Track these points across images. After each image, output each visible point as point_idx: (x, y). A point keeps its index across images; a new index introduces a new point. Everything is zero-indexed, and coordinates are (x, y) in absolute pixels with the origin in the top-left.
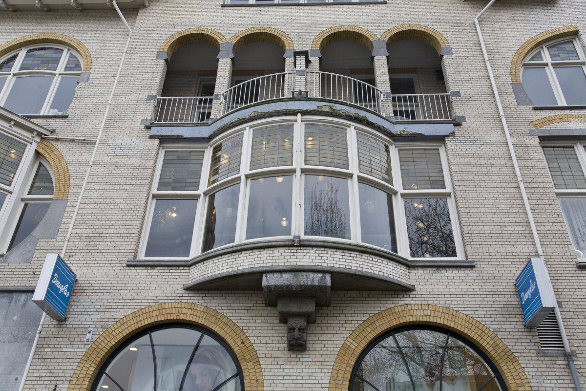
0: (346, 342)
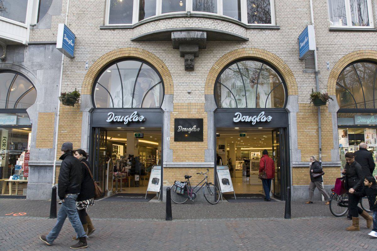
0: (214, 66)
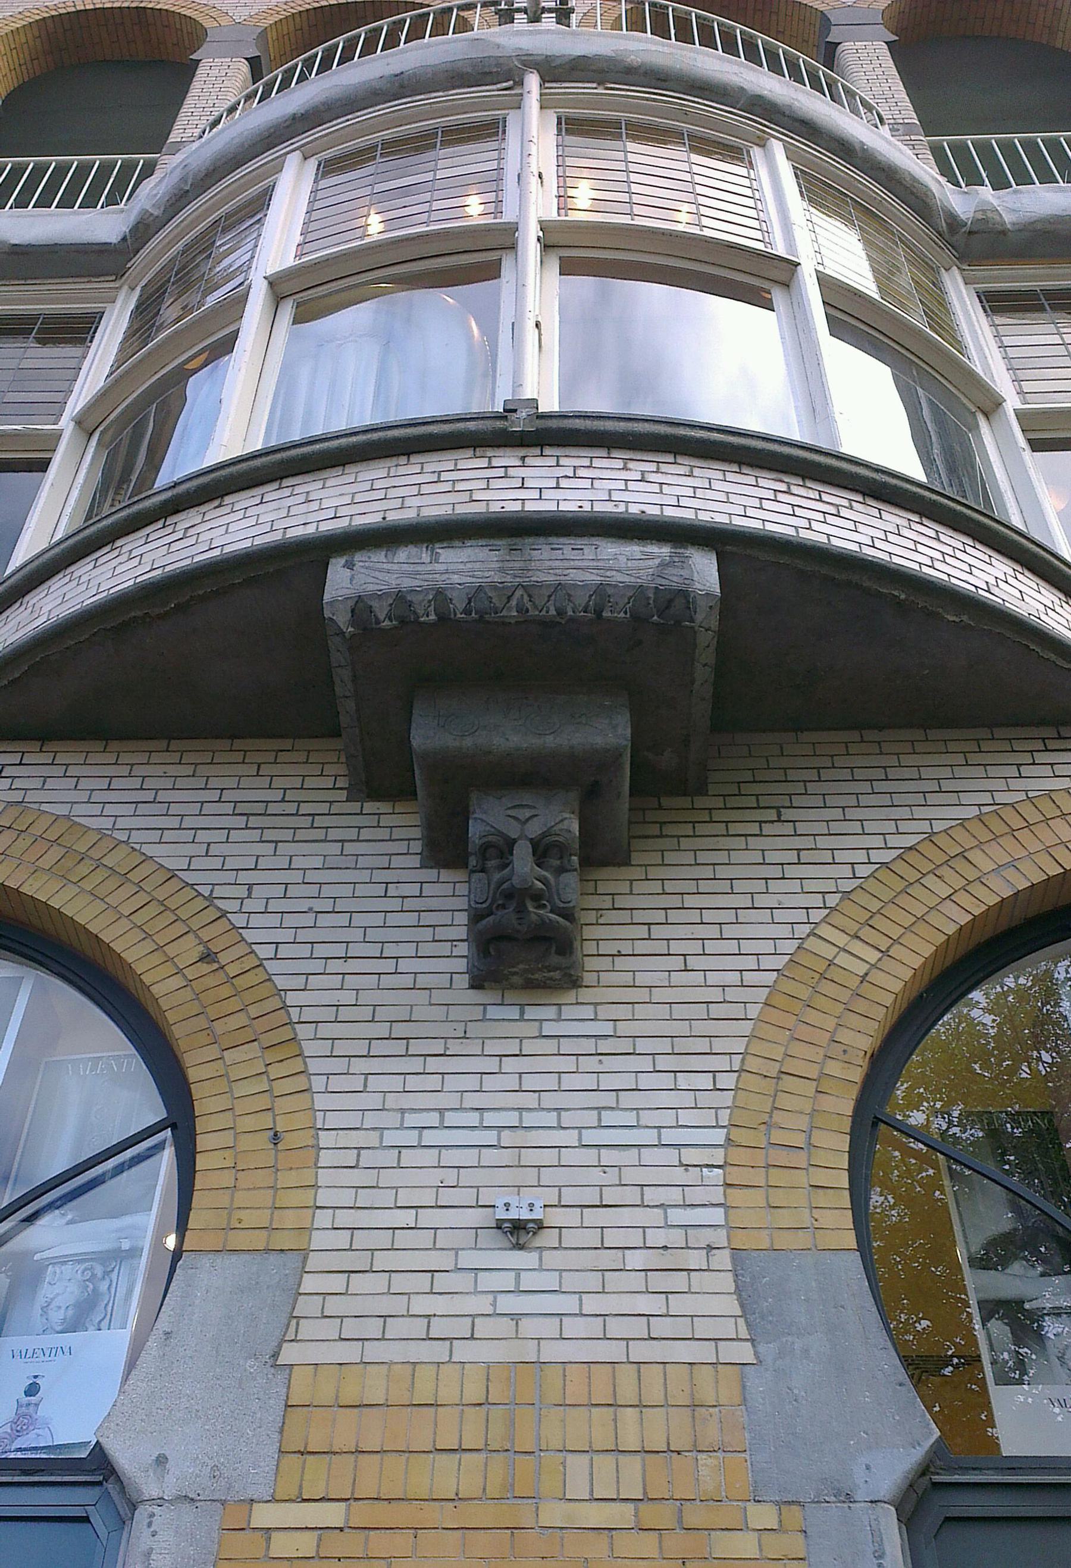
0: (812, 944)
